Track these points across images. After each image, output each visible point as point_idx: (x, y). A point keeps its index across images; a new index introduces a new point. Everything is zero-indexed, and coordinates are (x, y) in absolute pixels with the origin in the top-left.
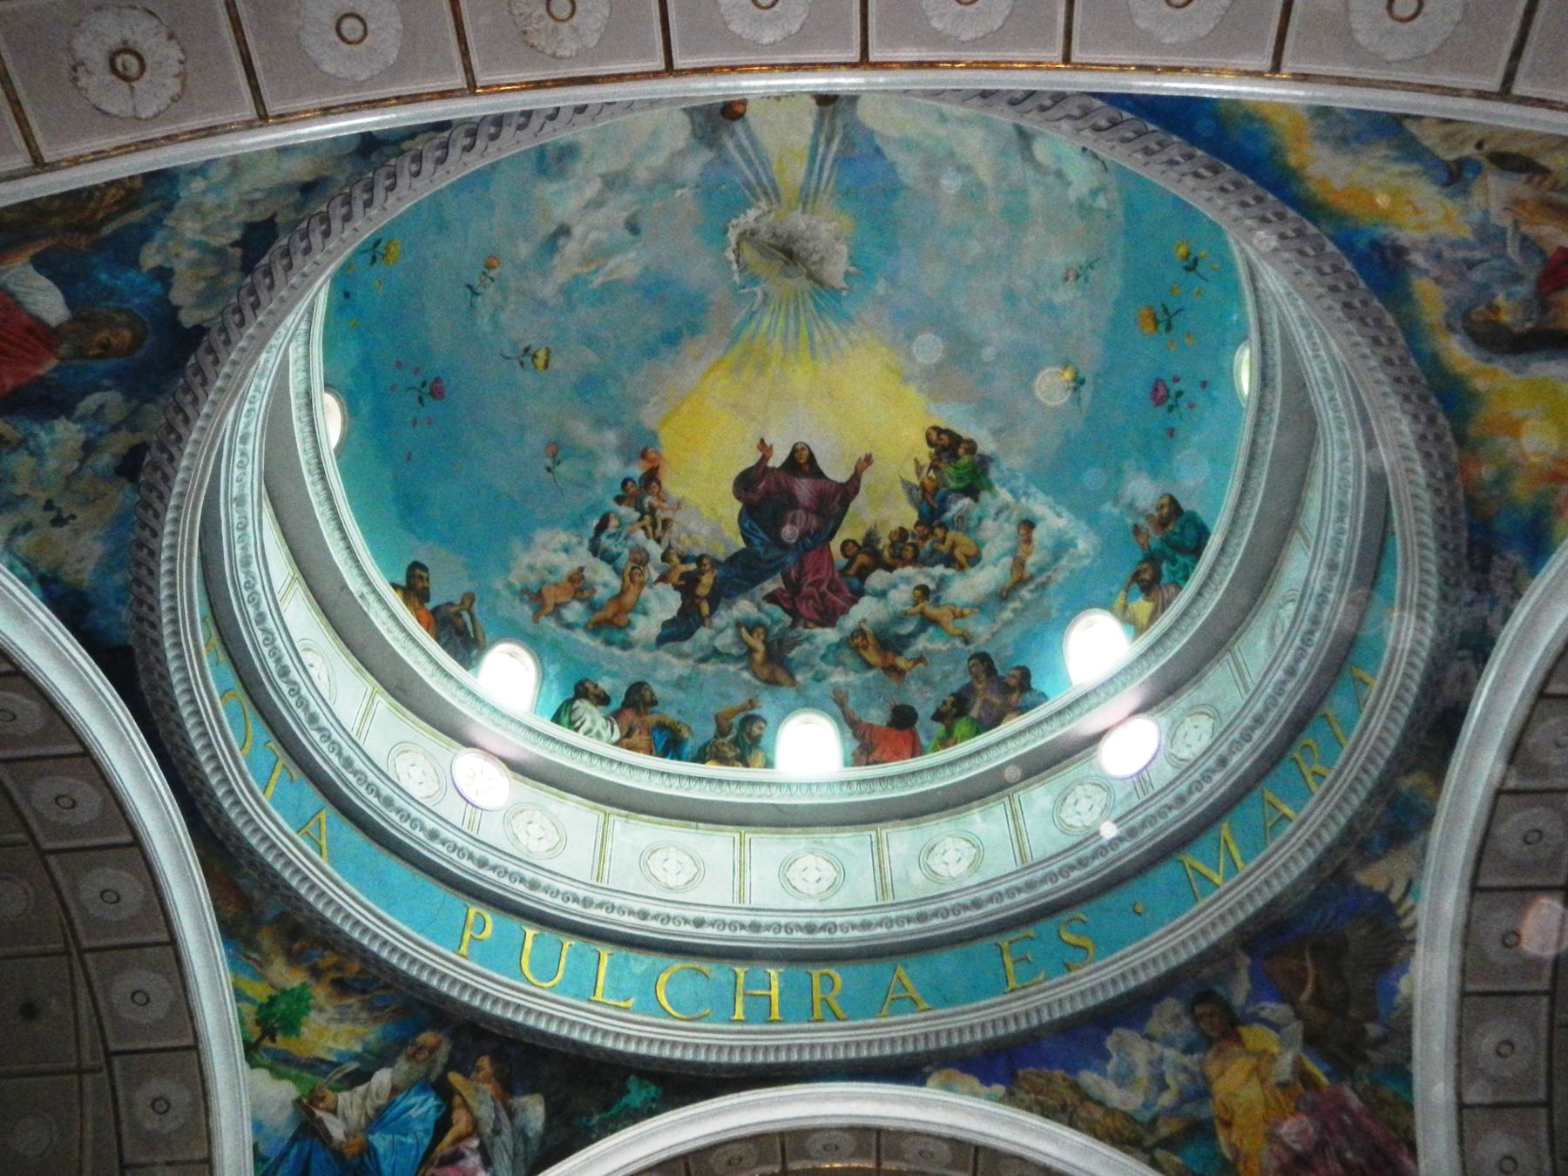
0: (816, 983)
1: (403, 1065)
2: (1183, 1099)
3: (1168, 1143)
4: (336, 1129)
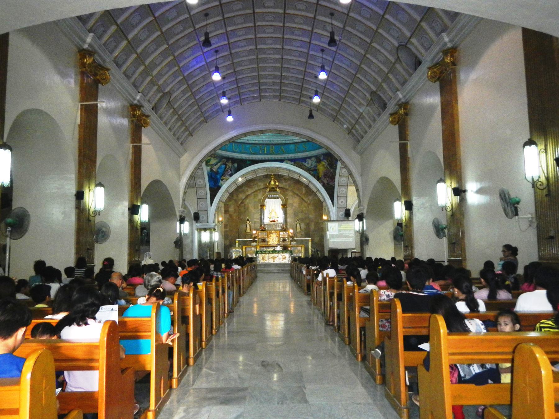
1: (221, 163)
3: (312, 171)
4: (214, 170)
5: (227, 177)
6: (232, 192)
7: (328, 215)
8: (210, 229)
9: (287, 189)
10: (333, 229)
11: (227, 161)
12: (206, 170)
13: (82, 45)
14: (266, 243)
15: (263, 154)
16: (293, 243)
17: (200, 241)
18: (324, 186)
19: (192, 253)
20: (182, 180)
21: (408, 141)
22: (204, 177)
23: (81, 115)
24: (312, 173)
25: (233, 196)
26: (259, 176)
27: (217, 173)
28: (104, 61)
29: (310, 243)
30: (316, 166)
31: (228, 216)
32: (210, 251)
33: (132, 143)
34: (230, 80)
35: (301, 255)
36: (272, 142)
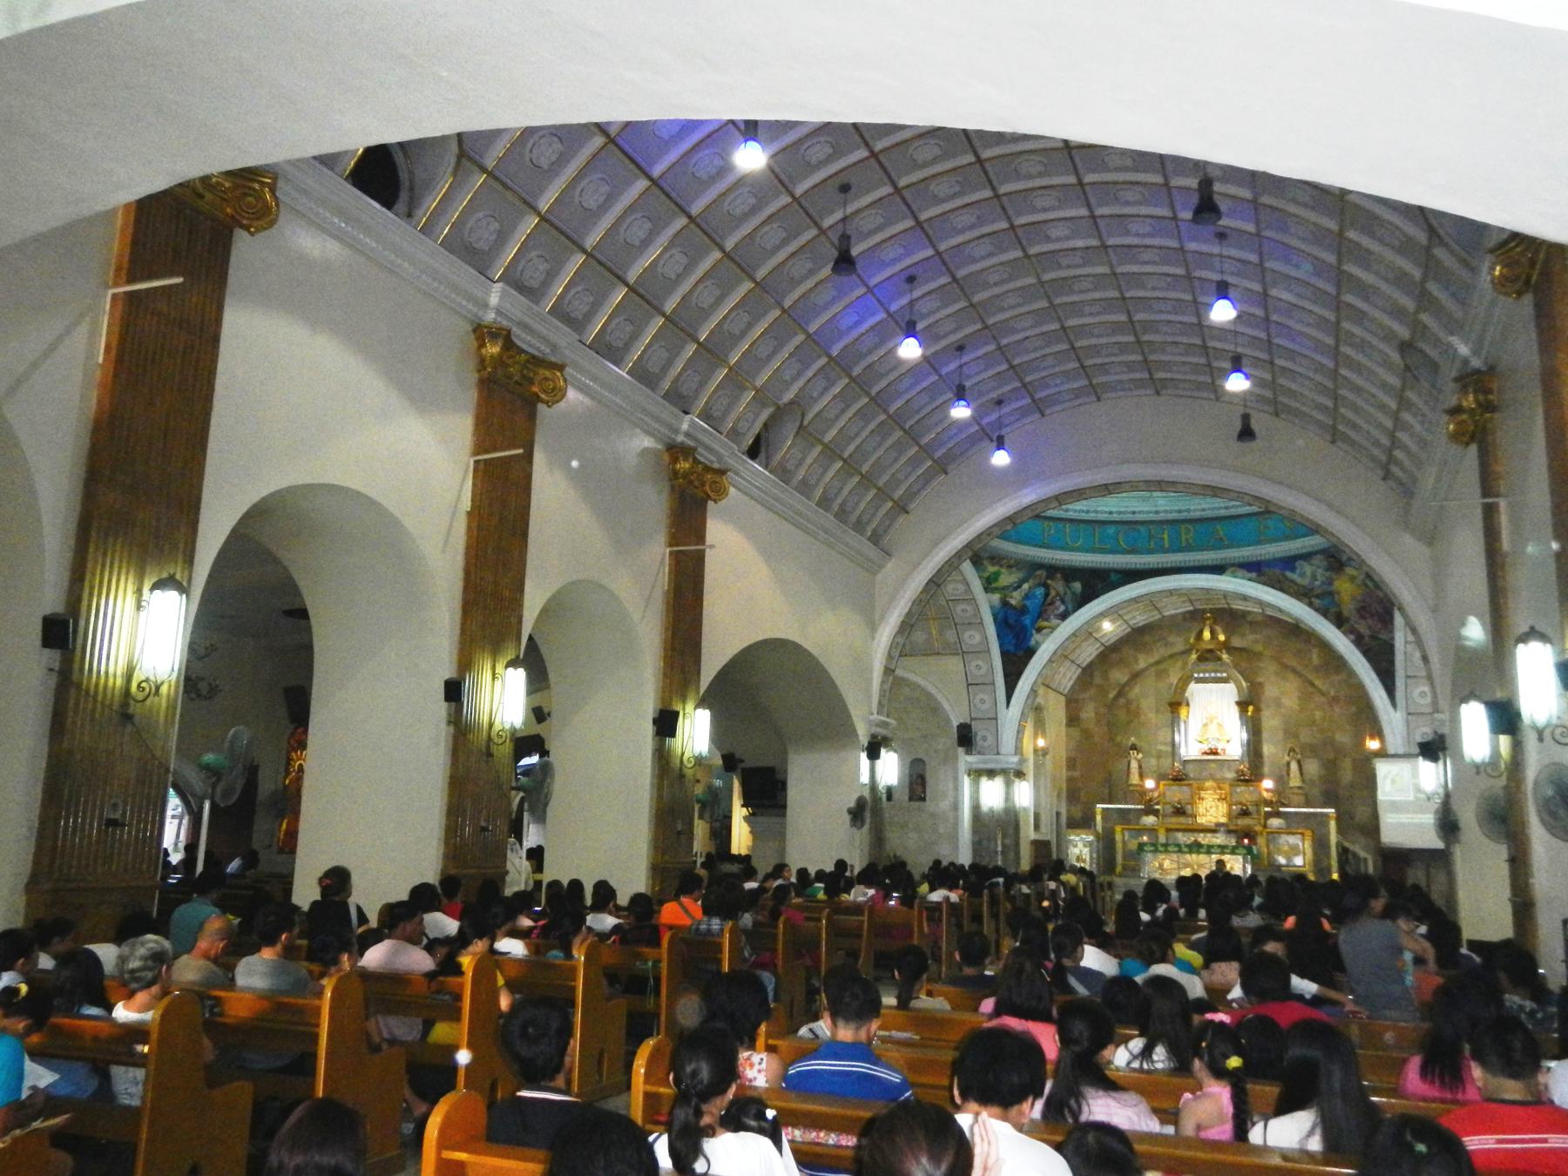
0: (1183, 532)
1: (1031, 581)
2: (1323, 583)
3: (1317, 596)
4: (1013, 602)
5: (1054, 621)
6: (1091, 665)
7: (1378, 733)
8: (1004, 772)
9: (1258, 656)
10: (1393, 782)
11: (1051, 576)
12: (986, 604)
13: (481, 313)
14: (1190, 821)
15: (1161, 550)
16: (1275, 822)
17: (976, 808)
18: (1359, 642)
19: (954, 837)
20: (878, 636)
21: (1497, 496)
22: (981, 623)
23: (474, 485)
24: (1317, 602)
25: (1091, 676)
26: (1172, 616)
27: (1023, 610)
28: (554, 347)
29: (1333, 824)
30: (1330, 582)
31: (1076, 733)
32: (1004, 837)
33: (671, 545)
34: (981, 352)
35: (1298, 861)
36: (1184, 515)
